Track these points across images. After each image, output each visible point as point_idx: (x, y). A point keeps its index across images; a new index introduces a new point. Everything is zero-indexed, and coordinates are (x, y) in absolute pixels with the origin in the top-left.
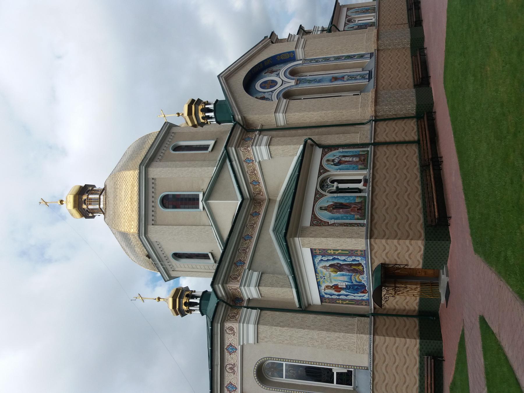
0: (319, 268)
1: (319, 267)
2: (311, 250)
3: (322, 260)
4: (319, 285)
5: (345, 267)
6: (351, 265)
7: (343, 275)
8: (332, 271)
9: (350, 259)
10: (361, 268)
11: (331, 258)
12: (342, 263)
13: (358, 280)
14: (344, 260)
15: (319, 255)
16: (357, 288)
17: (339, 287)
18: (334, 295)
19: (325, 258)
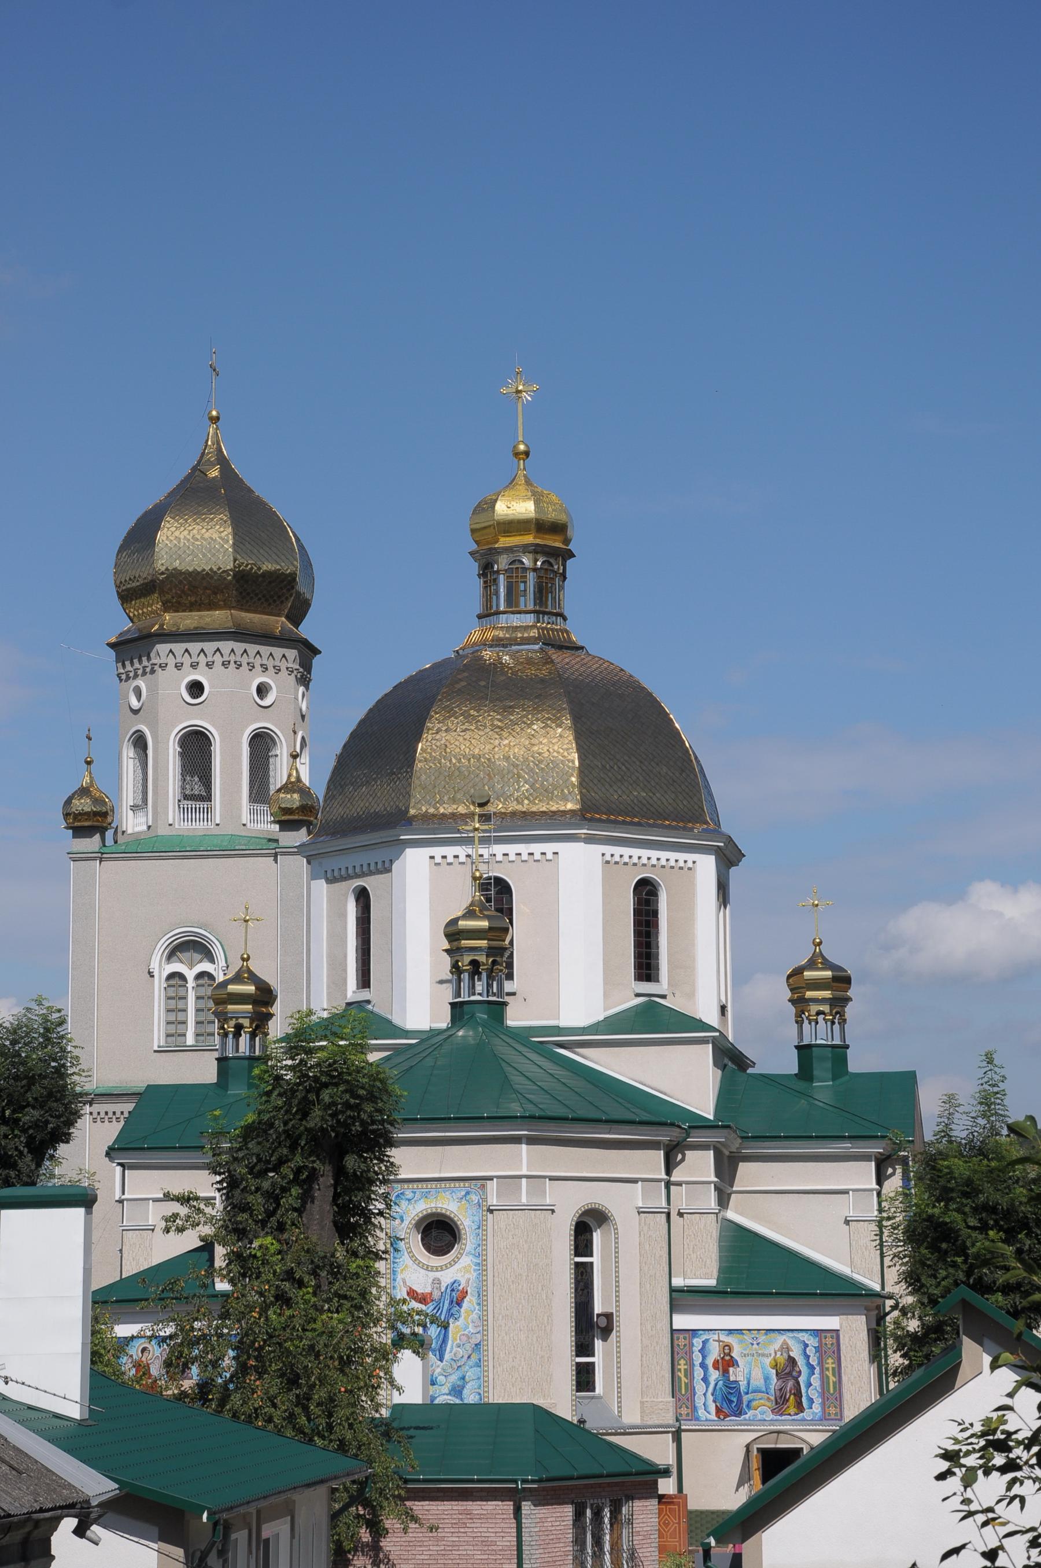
0: (781, 1339)
1: (784, 1337)
2: (838, 1330)
3: (806, 1346)
4: (731, 1331)
5: (790, 1384)
6: (798, 1394)
7: (767, 1379)
8: (775, 1360)
9: (813, 1394)
10: (792, 1410)
11: (814, 1361)
12: (802, 1380)
13: (754, 1404)
14: (809, 1385)
15: (820, 1342)
16: (731, 1402)
17: (731, 1370)
18: (704, 1357)
19: (811, 1351)
